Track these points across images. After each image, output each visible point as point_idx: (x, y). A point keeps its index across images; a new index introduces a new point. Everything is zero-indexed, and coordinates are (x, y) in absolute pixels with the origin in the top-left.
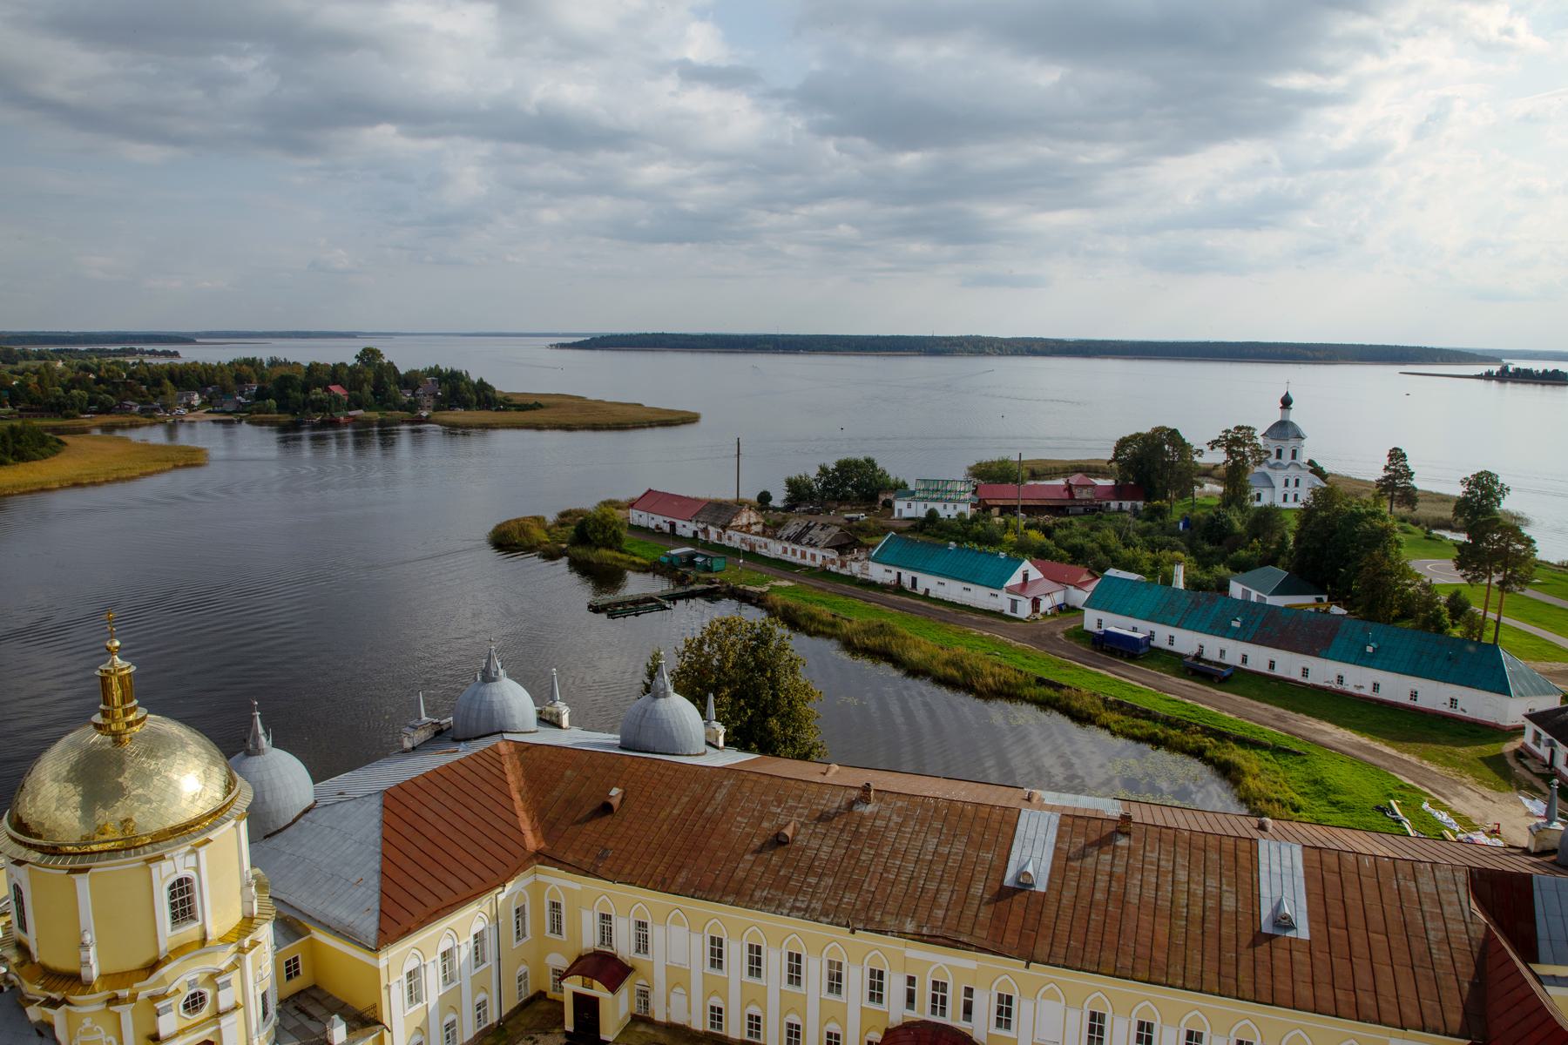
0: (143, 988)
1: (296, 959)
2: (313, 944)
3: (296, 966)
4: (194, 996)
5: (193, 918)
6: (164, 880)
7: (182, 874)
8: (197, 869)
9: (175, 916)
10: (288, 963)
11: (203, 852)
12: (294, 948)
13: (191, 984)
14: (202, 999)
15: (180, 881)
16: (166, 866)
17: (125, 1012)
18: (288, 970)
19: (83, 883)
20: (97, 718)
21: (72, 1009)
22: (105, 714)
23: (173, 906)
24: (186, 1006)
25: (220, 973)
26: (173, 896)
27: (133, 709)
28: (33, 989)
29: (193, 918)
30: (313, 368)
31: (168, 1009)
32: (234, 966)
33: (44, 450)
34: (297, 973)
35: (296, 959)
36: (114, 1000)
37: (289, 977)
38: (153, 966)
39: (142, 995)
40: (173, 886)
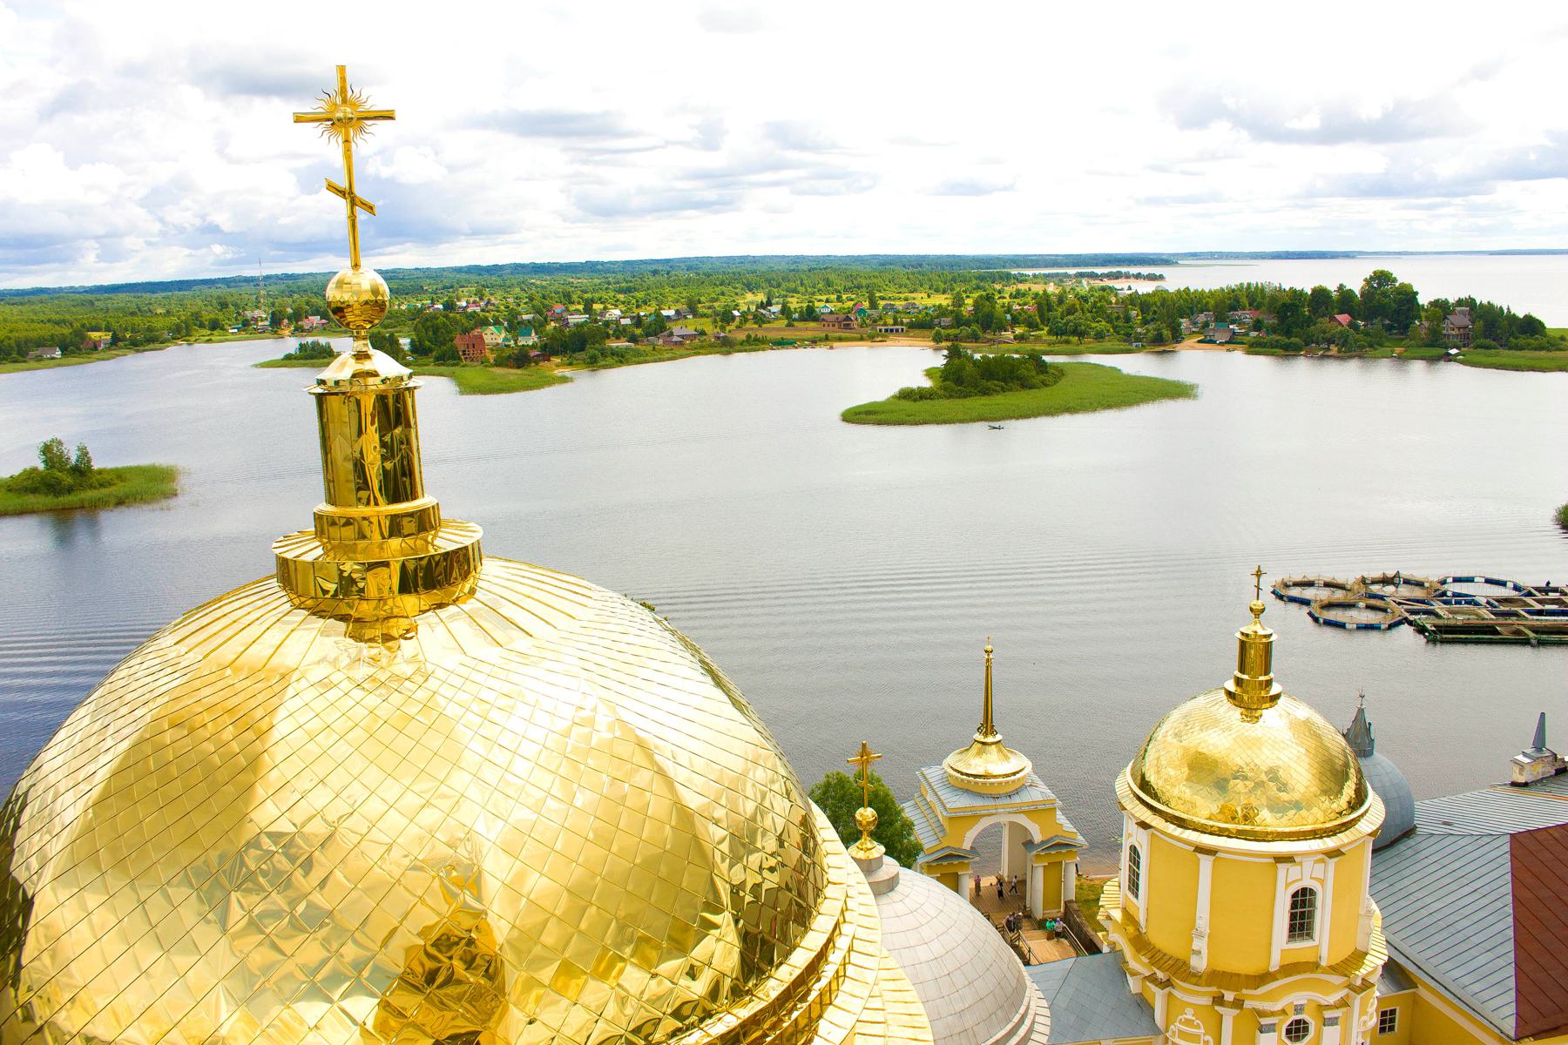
0: (1253, 997)
1: (1393, 1012)
2: (1416, 1001)
3: (1392, 1020)
4: (1298, 1022)
5: (1310, 936)
6: (1287, 885)
7: (1307, 883)
8: (1322, 882)
9: (1292, 928)
10: (1384, 1014)
11: (1332, 862)
12: (1399, 1001)
13: (1299, 1009)
14: (1306, 1029)
15: (1304, 891)
16: (1294, 871)
17: (1229, 1015)
18: (1382, 1022)
19: (1206, 862)
20: (1231, 686)
21: (1175, 992)
22: (1239, 682)
23: (1293, 917)
24: (1288, 1031)
25: (1328, 1007)
26: (1294, 905)
27: (1269, 683)
28: (1137, 963)
29: (1310, 936)
30: (1320, 295)
31: (1271, 1028)
32: (1344, 1003)
33: (1042, 377)
34: (1392, 1028)
35: (1393, 1012)
36: (1219, 1000)
37: (1382, 1030)
38: (1264, 978)
39: (1248, 1004)
40: (1295, 895)
